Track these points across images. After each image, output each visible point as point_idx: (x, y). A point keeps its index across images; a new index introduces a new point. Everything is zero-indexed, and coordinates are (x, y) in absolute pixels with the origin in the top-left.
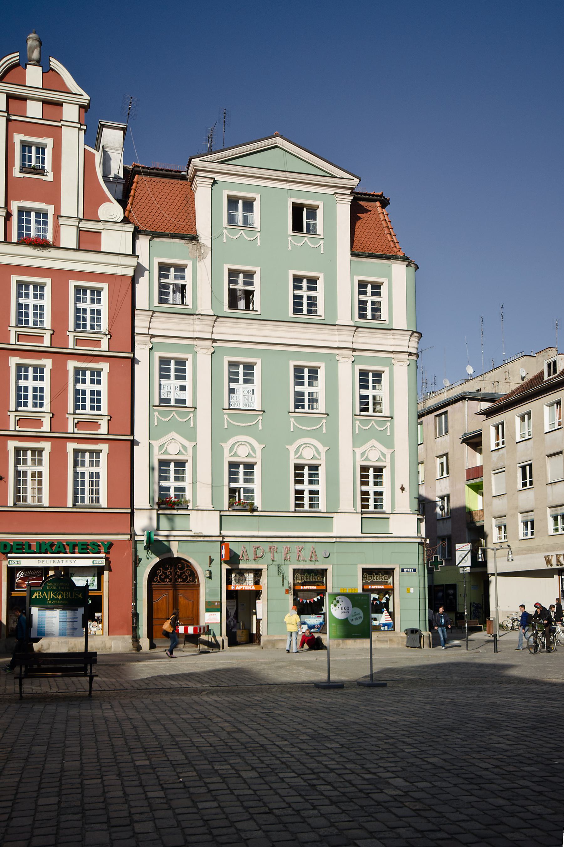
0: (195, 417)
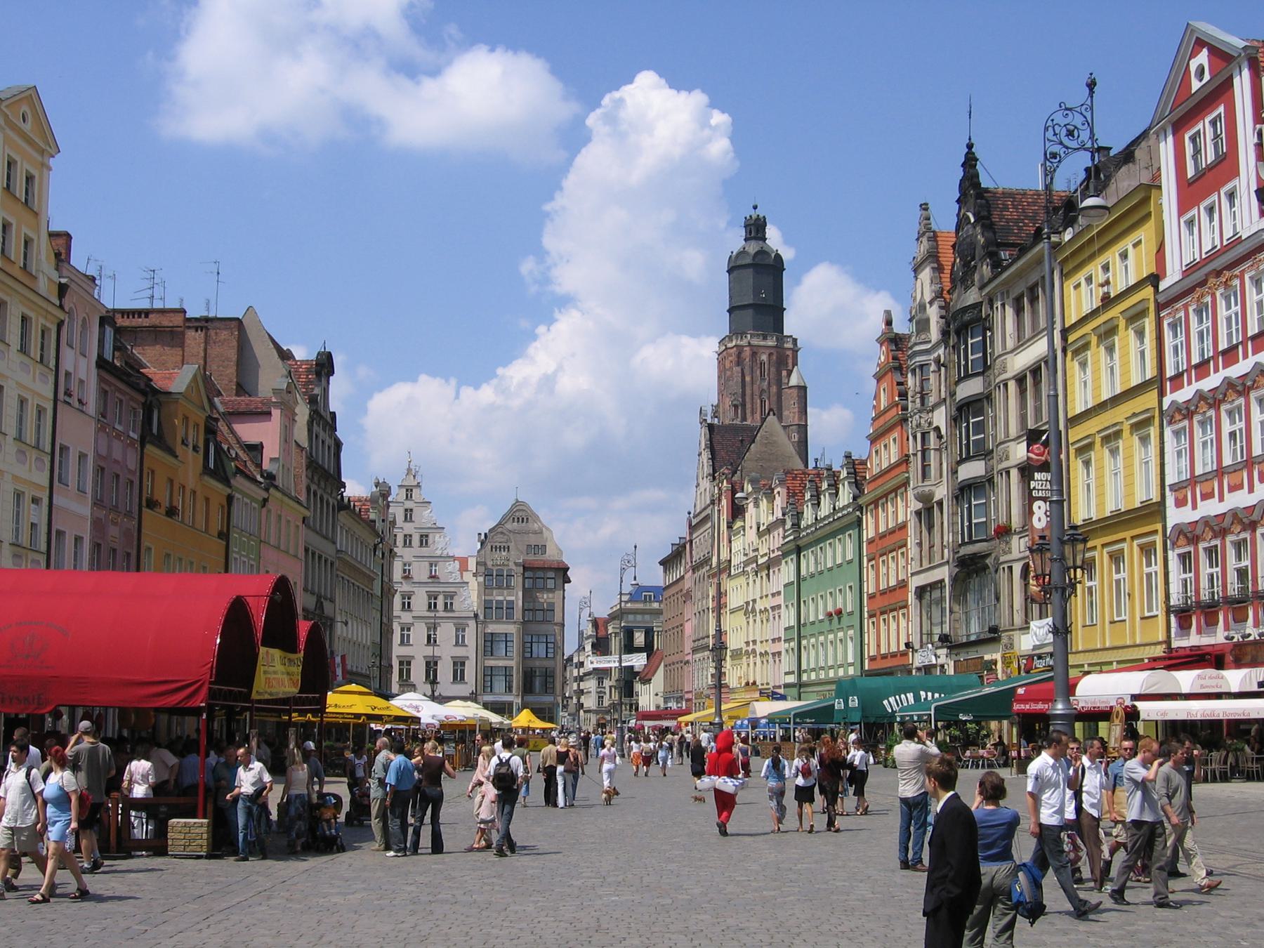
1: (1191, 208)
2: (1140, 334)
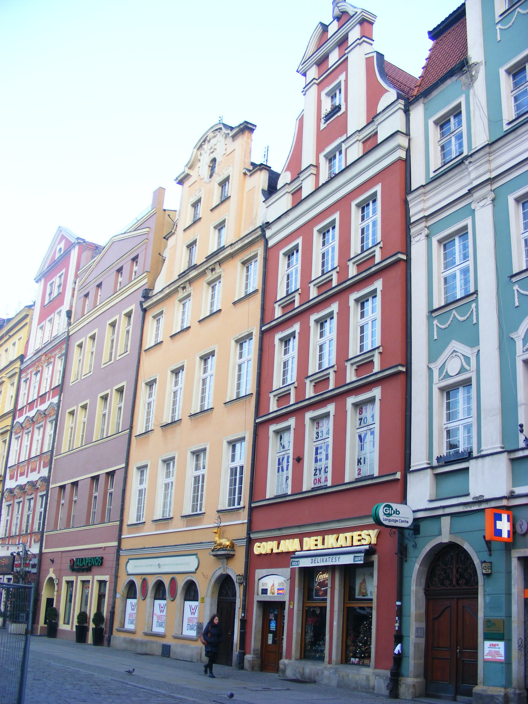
0: (477, 307)
1: (43, 321)
2: (13, 384)
